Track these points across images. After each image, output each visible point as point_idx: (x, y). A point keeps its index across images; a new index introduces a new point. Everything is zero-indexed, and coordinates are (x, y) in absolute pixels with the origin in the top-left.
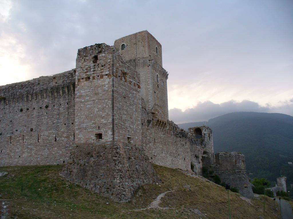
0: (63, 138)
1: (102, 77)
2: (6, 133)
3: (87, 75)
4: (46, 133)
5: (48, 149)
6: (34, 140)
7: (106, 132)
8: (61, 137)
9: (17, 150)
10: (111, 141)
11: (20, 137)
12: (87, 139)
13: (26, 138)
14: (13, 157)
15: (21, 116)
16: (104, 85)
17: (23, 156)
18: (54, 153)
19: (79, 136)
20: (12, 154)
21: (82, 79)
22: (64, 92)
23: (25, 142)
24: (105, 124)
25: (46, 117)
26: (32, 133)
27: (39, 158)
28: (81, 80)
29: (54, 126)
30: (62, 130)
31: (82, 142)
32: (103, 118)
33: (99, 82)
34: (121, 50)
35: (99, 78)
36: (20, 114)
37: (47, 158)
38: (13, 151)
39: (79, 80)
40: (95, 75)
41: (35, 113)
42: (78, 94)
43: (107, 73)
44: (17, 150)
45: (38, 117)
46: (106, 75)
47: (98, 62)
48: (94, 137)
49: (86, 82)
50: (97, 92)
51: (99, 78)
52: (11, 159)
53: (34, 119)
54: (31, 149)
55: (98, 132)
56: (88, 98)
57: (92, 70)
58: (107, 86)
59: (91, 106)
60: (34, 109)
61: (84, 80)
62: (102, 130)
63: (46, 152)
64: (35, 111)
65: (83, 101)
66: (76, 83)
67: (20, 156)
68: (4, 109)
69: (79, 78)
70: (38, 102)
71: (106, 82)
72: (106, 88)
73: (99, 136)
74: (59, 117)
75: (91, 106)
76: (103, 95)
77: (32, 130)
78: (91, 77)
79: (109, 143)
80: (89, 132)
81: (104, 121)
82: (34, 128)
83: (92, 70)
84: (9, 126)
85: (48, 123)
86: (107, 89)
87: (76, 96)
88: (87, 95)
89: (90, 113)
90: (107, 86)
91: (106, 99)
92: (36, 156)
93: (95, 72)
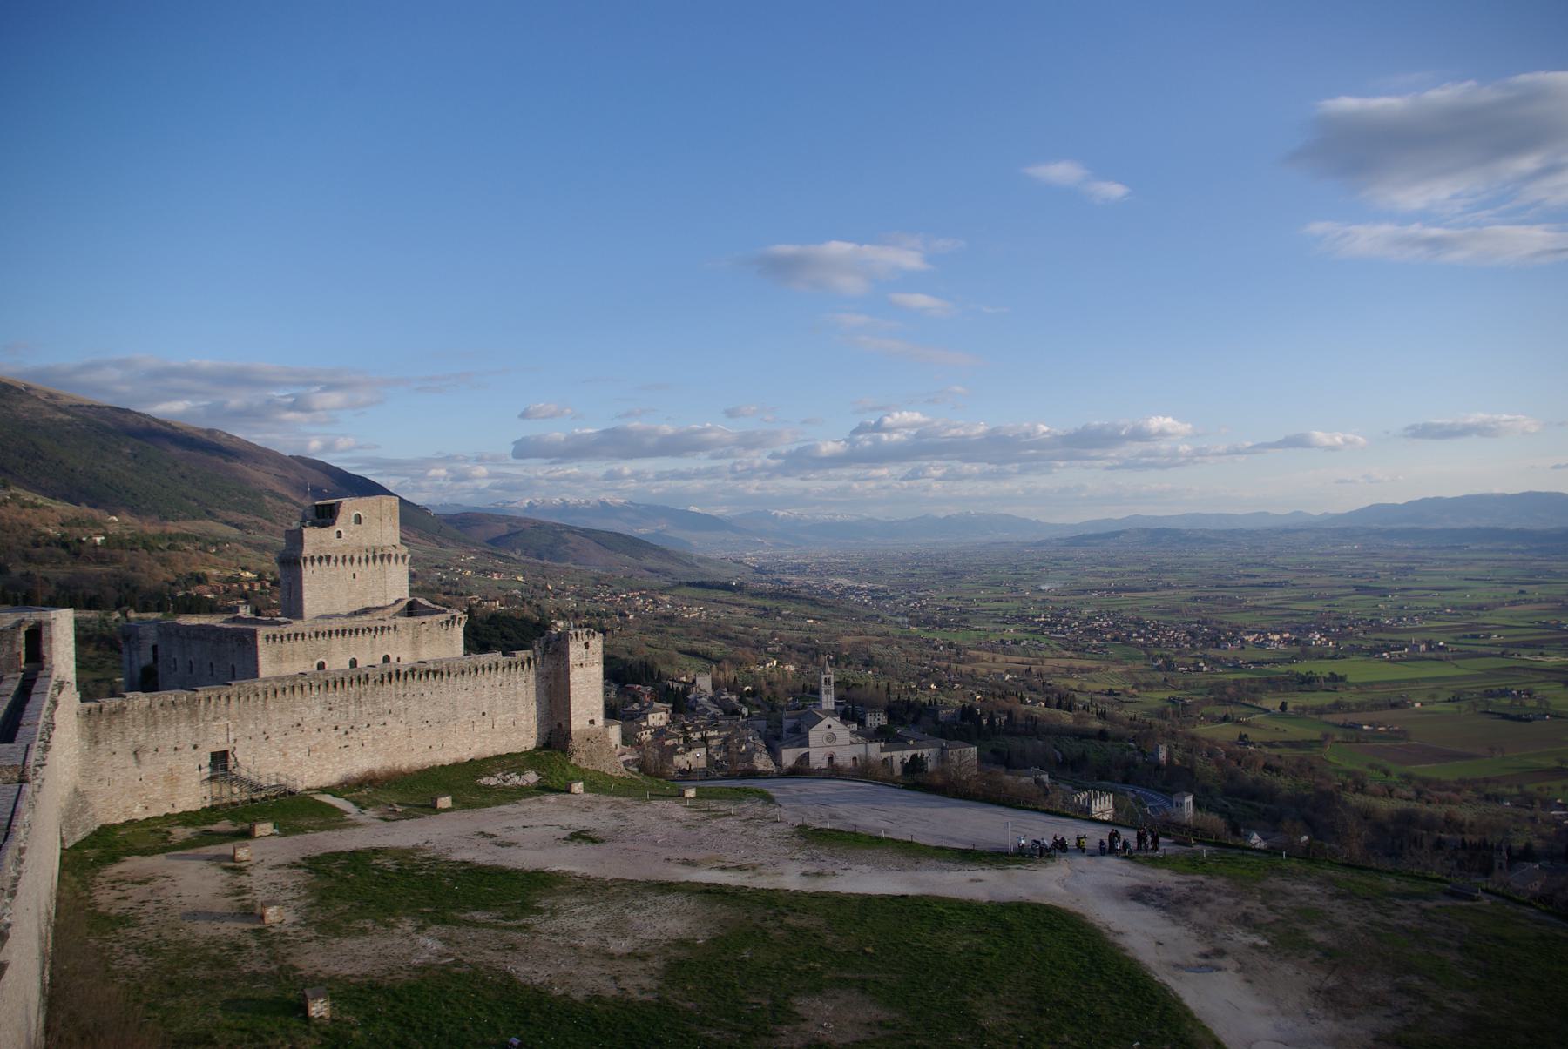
6: (487, 726)
13: (478, 724)
22: (523, 668)
36: (465, 694)
41: (486, 692)
54: (485, 738)
55: (591, 718)
63: (503, 740)
72: (597, 676)
77: (484, 714)
81: (596, 708)
82: (486, 711)
85: (503, 705)
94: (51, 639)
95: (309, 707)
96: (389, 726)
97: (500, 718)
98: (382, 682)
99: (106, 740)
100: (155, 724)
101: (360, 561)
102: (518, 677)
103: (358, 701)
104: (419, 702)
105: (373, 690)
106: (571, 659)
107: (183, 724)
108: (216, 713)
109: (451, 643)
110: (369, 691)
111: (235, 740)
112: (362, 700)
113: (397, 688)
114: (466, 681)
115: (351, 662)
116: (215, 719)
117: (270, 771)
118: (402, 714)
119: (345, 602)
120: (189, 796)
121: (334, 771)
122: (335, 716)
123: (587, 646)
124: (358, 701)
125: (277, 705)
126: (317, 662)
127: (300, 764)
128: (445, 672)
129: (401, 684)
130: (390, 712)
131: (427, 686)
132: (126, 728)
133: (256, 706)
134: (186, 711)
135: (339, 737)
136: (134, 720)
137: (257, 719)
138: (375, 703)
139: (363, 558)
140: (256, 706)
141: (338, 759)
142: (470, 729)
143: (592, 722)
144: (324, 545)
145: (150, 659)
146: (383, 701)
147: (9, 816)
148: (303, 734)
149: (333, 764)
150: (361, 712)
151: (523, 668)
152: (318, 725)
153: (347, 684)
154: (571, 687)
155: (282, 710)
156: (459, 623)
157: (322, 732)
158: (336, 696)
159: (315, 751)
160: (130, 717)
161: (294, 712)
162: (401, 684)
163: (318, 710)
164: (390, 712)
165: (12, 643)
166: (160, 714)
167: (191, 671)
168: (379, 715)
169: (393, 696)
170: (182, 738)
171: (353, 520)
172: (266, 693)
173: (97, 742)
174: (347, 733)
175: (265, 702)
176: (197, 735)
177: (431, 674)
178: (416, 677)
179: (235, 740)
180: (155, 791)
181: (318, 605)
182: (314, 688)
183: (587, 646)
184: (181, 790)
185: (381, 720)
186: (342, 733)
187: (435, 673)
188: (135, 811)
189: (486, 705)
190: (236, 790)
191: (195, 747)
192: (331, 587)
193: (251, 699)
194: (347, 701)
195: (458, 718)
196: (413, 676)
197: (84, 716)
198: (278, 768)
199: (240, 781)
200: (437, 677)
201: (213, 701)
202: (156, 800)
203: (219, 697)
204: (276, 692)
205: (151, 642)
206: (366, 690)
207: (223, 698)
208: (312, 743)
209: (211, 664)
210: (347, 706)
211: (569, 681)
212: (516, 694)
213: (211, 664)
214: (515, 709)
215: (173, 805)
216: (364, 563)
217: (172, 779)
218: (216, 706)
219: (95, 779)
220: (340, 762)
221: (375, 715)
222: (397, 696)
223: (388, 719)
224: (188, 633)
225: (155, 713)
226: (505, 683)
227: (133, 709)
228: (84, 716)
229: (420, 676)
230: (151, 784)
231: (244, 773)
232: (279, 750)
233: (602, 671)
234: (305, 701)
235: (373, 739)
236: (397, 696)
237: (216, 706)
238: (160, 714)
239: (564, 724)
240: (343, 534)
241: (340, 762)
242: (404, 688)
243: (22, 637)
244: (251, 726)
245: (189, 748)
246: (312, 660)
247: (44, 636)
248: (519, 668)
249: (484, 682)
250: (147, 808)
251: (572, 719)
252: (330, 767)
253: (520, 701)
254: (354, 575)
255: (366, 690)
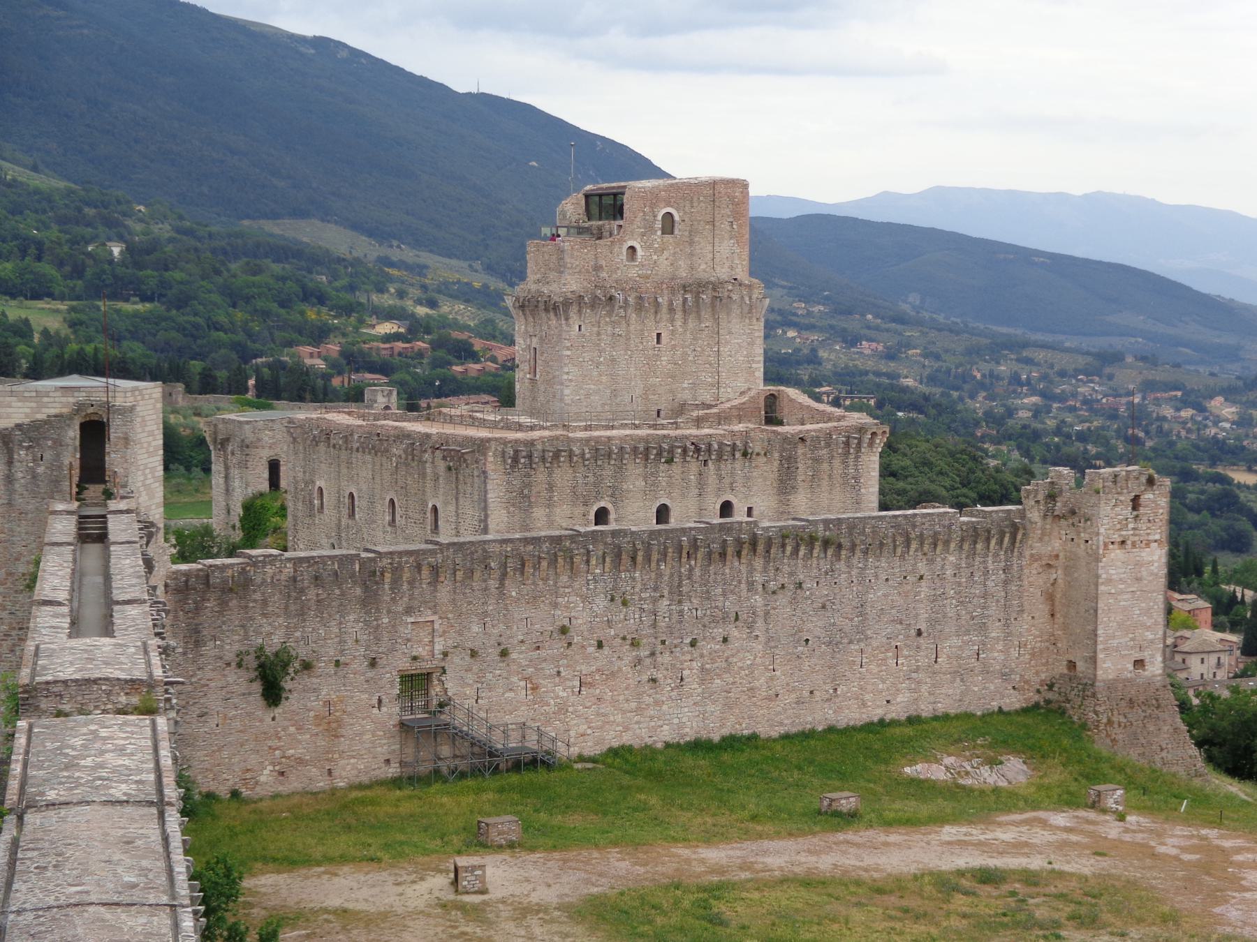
0: (996, 654)
1: (1148, 545)
2: (846, 641)
3: (1120, 536)
4: (956, 641)
5: (962, 680)
6: (924, 660)
7: (1152, 656)
8: (992, 650)
9: (881, 686)
10: (1160, 675)
11: (887, 651)
12: (1118, 670)
14: (870, 704)
15: (884, 595)
16: (1151, 563)
17: (898, 700)
18: (976, 689)
19: (1104, 666)
20: (867, 697)
21: (1112, 543)
22: (1000, 542)
23: (903, 664)
24: (1152, 641)
25: (954, 601)
26: (921, 640)
27: (940, 702)
28: (1111, 547)
29: (975, 624)
30: (993, 635)
31: (1111, 677)
32: (1148, 628)
33: (1143, 554)
34: (659, 233)
35: (1143, 545)
37: (960, 700)
38: (870, 688)
39: (1106, 545)
40: (1136, 538)
41: (924, 589)
42: (1104, 576)
43: (1157, 537)
44: (881, 686)
45: (934, 599)
46: (1156, 541)
47: (1142, 510)
48: (1131, 667)
49: (1118, 551)
50: (1139, 575)
51: (1143, 545)
52: (864, 710)
53: (922, 606)
55: (1138, 656)
56: (1123, 586)
57: (1131, 526)
58: (1156, 564)
59: (1129, 603)
60: (921, 578)
61: (1116, 546)
62: (1146, 653)
64: (923, 583)
65: (1113, 591)
66: (1101, 552)
67: (888, 702)
68: (833, 571)
69: (1107, 540)
70: (931, 561)
71: (1156, 558)
72: (1154, 568)
73: (1139, 663)
74: (985, 603)
75: (1129, 603)
76: (1150, 582)
77: (919, 633)
78: (1129, 542)
79: (1159, 678)
80: (1123, 656)
81: (1150, 636)
82: (923, 627)
83: (1131, 526)
84: (851, 620)
86: (1156, 571)
87: (1100, 581)
88: (1121, 580)
89: (1125, 618)
90: (1156, 564)
91: (1154, 591)
92: (932, 699)
93: (1137, 532)
94: (126, 440)
95: (585, 599)
96: (734, 644)
97: (951, 644)
98: (723, 555)
99: (214, 638)
100: (302, 614)
101: (671, 310)
102: (990, 559)
103: (678, 595)
104: (794, 601)
105: (705, 570)
106: (1102, 530)
107: (351, 618)
108: (411, 597)
109: (853, 484)
110: (697, 572)
111: (445, 654)
112: (685, 589)
113: (750, 564)
114: (883, 566)
115: (658, 511)
116: (409, 611)
117: (508, 719)
118: (760, 623)
119: (638, 391)
120: (359, 756)
121: (626, 729)
122: (630, 620)
123: (1136, 503)
124: (678, 595)
125: (525, 589)
126: (602, 504)
127: (562, 709)
128: (845, 542)
129: (759, 563)
130: (737, 619)
131: (809, 569)
132: (251, 619)
133: (486, 589)
134: (358, 591)
135: (638, 661)
136: (265, 603)
137: (485, 614)
138: (707, 596)
139: (678, 302)
140: (486, 589)
141: (633, 705)
142: (892, 662)
143: (1139, 663)
144: (604, 275)
145: (264, 486)
146: (724, 594)
147: (152, 777)
148: (569, 652)
149: (624, 712)
150: (681, 613)
151: (1000, 542)
152: (599, 634)
153: (655, 557)
154: (1102, 588)
155: (534, 600)
156: (871, 444)
157: (606, 650)
158: (636, 580)
159: (591, 685)
160: (258, 596)
161: (555, 605)
162: (759, 563)
163: (601, 603)
164: (737, 619)
165: (58, 443)
166: (312, 594)
167: (352, 514)
168: (714, 620)
169: (743, 586)
170: (350, 643)
171: (659, 225)
172: (505, 566)
173: (198, 644)
174: (653, 654)
175: (502, 585)
176: (378, 639)
177: (818, 544)
178: (789, 549)
179: (445, 654)
180: (300, 742)
181: (588, 395)
182: (593, 562)
183: (1136, 503)
184: (344, 744)
185: (719, 632)
186: (644, 653)
187: (826, 543)
188: (263, 779)
189: (924, 616)
190: (445, 751)
191: (373, 663)
192: (613, 360)
193: (477, 575)
194: (655, 589)
195: (867, 638)
196: (783, 546)
197: (178, 591)
198: (522, 714)
199: (457, 736)
200: (830, 552)
201: (406, 575)
202: (300, 761)
203: (419, 568)
204: (523, 565)
205: (266, 454)
206: (691, 570)
207: (425, 572)
208: (585, 669)
209: (392, 501)
210: (655, 601)
211: (1098, 576)
212: (985, 596)
213: (392, 501)
214: (983, 627)
215: (330, 772)
216: (679, 315)
217: (331, 724)
218: (411, 583)
219: (195, 711)
220: (639, 710)
221: (706, 620)
222: (751, 584)
223: (735, 633)
224: (346, 439)
225: (302, 591)
226: (965, 573)
227: (264, 581)
228: (178, 591)
229: (796, 551)
230: (292, 729)
231: (459, 720)
232: (526, 679)
233: (1164, 560)
234: (576, 585)
235: (702, 669)
236: (751, 584)
237: (411, 583)
238: (312, 594)
239: (1081, 666)
240: (640, 252)
241: (639, 710)
242: (765, 570)
243: (73, 434)
244: (476, 628)
245: (360, 665)
246: (585, 504)
247: (114, 433)
248: (993, 542)
249: (922, 567)
250: (282, 774)
251: (1101, 656)
252: (619, 718)
253: (993, 610)
254: (659, 335)
255: (691, 570)
